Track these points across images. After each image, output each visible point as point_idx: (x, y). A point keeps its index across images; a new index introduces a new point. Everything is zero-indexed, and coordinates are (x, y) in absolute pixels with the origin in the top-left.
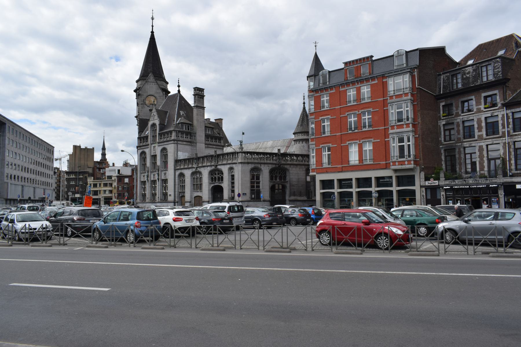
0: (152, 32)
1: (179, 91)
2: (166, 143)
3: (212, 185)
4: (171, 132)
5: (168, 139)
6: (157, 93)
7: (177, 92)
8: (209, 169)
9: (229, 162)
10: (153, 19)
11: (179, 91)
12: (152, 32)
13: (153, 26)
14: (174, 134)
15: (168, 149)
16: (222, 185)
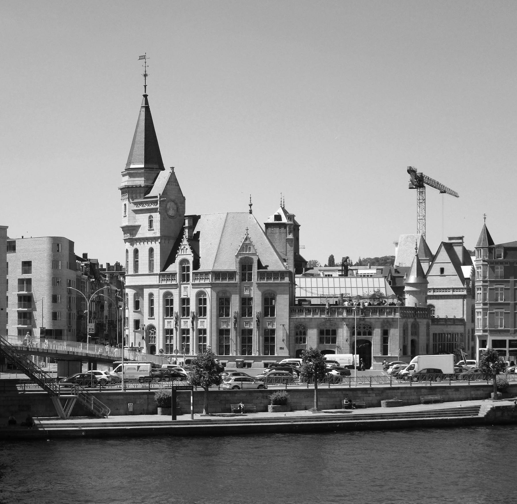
0: (145, 96)
10: (145, 75)
13: (145, 86)
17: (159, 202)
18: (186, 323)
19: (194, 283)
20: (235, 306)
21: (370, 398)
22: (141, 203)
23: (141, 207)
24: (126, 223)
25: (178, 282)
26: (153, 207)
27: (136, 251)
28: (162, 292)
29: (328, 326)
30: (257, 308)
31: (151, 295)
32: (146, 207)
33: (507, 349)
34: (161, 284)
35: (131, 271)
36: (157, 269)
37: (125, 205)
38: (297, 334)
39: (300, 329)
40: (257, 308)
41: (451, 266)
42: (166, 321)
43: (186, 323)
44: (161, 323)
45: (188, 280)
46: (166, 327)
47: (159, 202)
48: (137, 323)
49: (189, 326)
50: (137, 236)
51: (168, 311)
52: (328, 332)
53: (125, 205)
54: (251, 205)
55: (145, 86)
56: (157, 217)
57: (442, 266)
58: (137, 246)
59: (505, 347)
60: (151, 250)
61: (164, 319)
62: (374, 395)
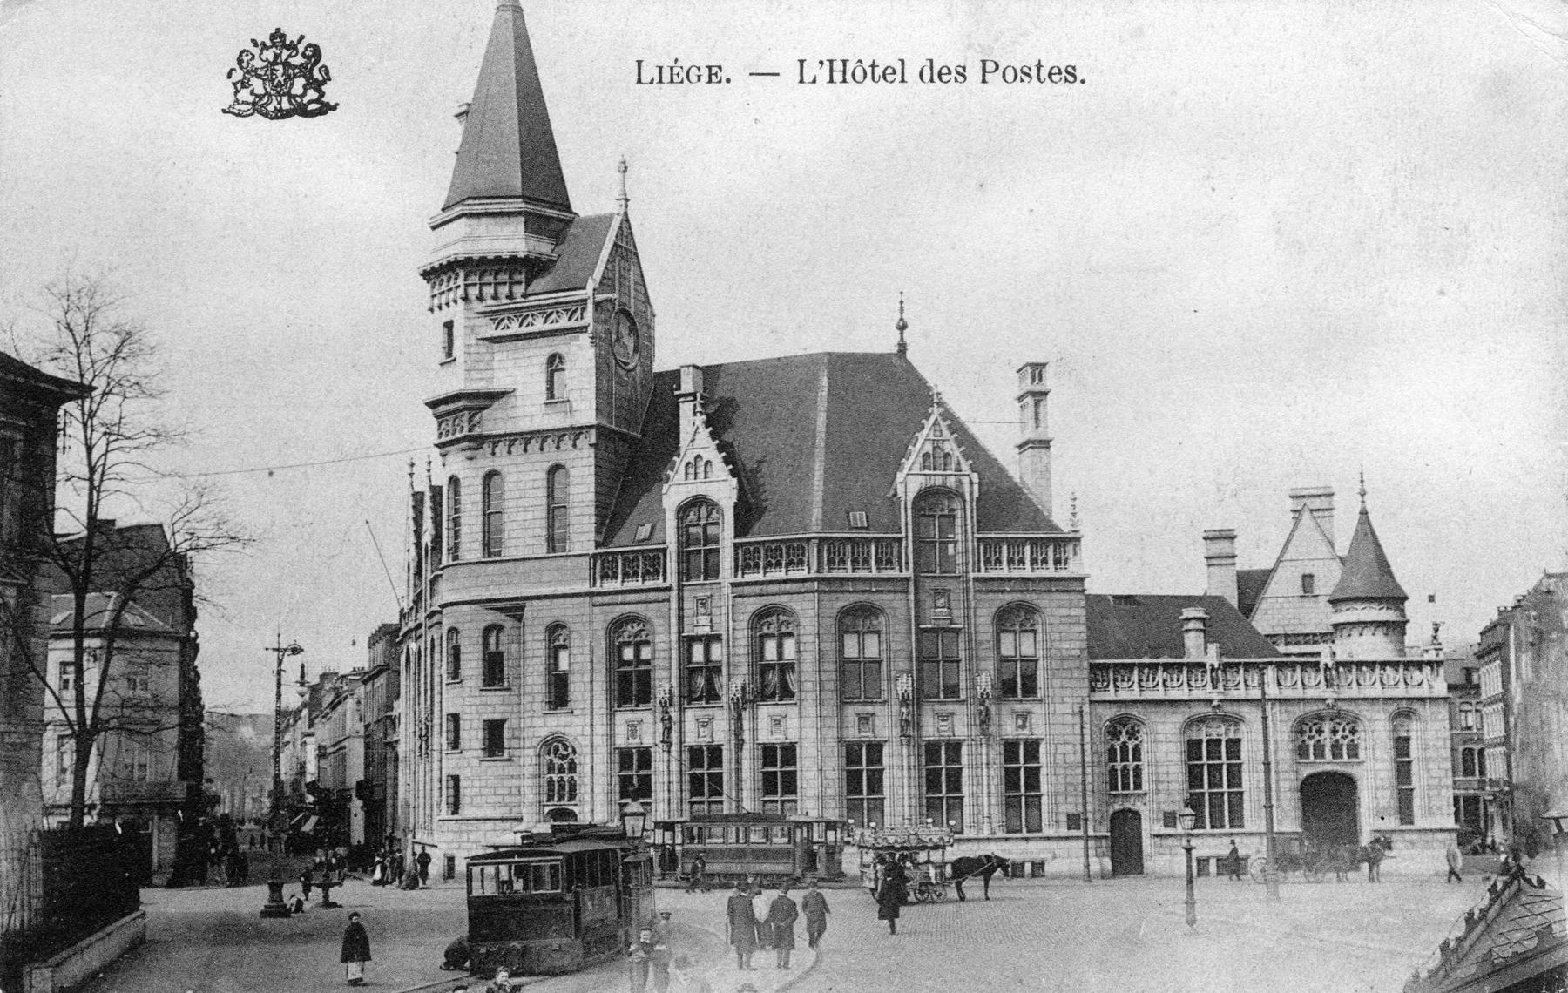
1: (902, 347)
5: (1049, 571)
7: (895, 350)
11: (902, 347)
17: (590, 307)
18: (706, 725)
19: (739, 579)
22: (520, 313)
23: (515, 328)
24: (454, 381)
25: (672, 579)
28: (602, 618)
31: (555, 628)
32: (539, 325)
34: (597, 589)
35: (471, 548)
36: (582, 534)
37: (449, 326)
39: (1124, 738)
42: (622, 718)
43: (706, 725)
44: (601, 729)
45: (711, 571)
46: (621, 742)
47: (590, 307)
48: (494, 734)
49: (721, 733)
51: (630, 686)
52: (1214, 744)
53: (449, 326)
54: (902, 327)
56: (581, 356)
58: (502, 461)
61: (611, 714)
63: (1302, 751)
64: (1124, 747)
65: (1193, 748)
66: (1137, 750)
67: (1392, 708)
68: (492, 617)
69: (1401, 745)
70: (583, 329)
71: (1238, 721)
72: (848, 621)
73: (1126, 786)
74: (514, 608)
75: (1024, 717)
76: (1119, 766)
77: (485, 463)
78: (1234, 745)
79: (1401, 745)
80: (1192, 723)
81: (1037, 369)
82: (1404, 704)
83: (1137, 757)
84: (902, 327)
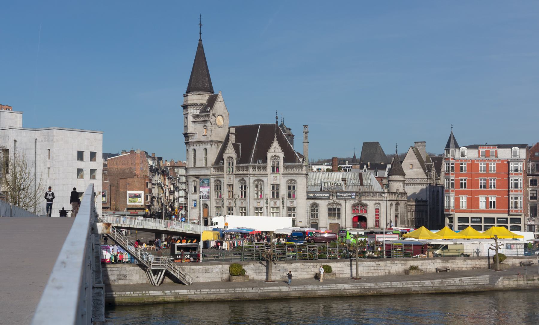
0: (200, 40)
1: (277, 123)
2: (294, 175)
3: (354, 215)
4: (301, 167)
5: (299, 172)
6: (224, 113)
8: (352, 202)
9: (375, 199)
10: (201, 25)
11: (277, 123)
12: (200, 40)
13: (200, 33)
14: (304, 169)
15: (297, 181)
16: (366, 216)
20: (267, 191)
21: (397, 268)
23: (198, 120)
26: (206, 119)
27: (195, 150)
29: (334, 206)
30: (283, 191)
32: (202, 119)
33: (483, 224)
38: (312, 211)
40: (283, 191)
41: (417, 162)
50: (194, 140)
52: (334, 209)
55: (200, 33)
57: (411, 162)
59: (484, 223)
60: (206, 149)
62: (400, 265)
63: (354, 210)
64: (314, 209)
65: (330, 209)
66: (317, 210)
67: (374, 202)
68: (195, 179)
69: (377, 210)
70: (209, 121)
71: (340, 204)
72: (256, 182)
73: (314, 217)
74: (197, 177)
75: (292, 203)
76: (316, 213)
77: (192, 148)
78: (339, 210)
79: (377, 210)
80: (329, 204)
81: (306, 127)
82: (377, 202)
83: (317, 211)
84: (277, 118)
